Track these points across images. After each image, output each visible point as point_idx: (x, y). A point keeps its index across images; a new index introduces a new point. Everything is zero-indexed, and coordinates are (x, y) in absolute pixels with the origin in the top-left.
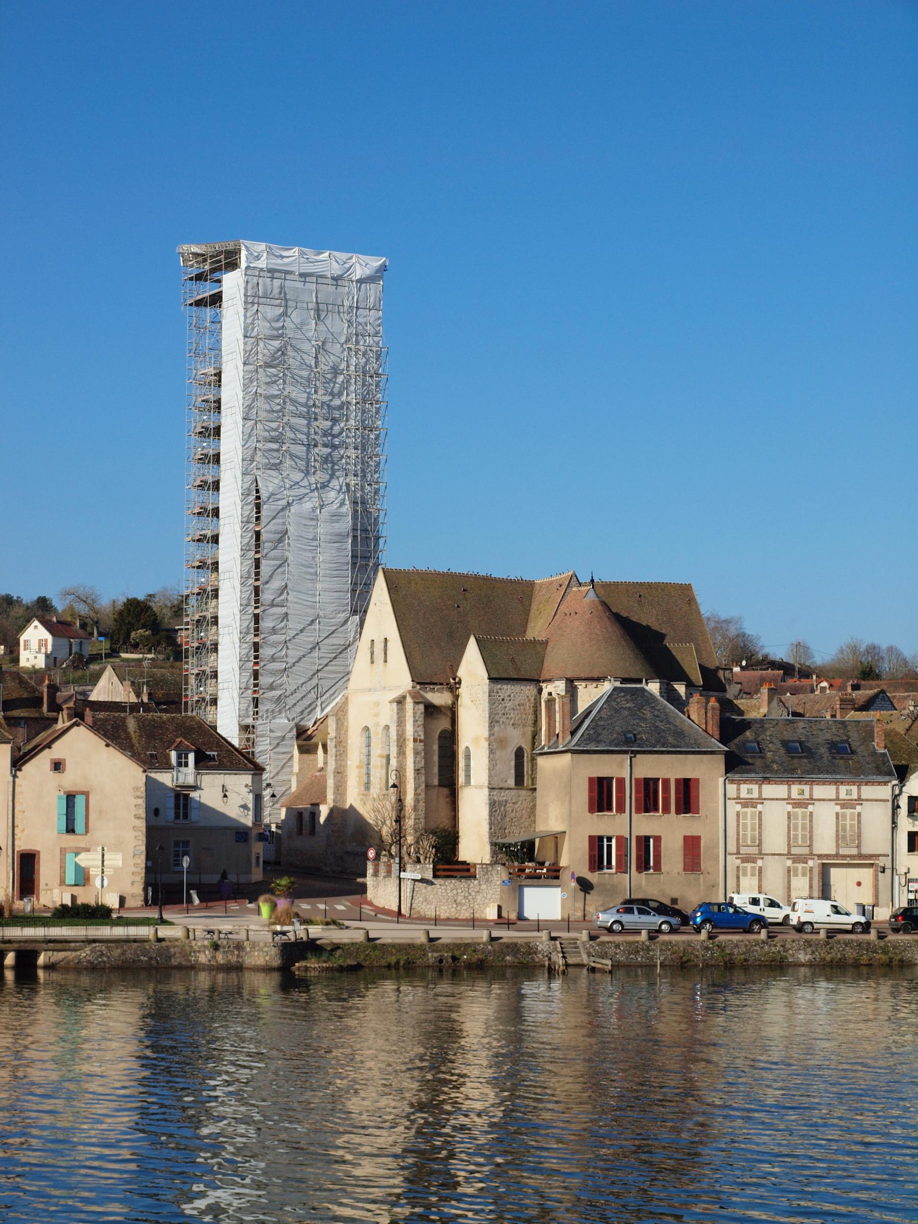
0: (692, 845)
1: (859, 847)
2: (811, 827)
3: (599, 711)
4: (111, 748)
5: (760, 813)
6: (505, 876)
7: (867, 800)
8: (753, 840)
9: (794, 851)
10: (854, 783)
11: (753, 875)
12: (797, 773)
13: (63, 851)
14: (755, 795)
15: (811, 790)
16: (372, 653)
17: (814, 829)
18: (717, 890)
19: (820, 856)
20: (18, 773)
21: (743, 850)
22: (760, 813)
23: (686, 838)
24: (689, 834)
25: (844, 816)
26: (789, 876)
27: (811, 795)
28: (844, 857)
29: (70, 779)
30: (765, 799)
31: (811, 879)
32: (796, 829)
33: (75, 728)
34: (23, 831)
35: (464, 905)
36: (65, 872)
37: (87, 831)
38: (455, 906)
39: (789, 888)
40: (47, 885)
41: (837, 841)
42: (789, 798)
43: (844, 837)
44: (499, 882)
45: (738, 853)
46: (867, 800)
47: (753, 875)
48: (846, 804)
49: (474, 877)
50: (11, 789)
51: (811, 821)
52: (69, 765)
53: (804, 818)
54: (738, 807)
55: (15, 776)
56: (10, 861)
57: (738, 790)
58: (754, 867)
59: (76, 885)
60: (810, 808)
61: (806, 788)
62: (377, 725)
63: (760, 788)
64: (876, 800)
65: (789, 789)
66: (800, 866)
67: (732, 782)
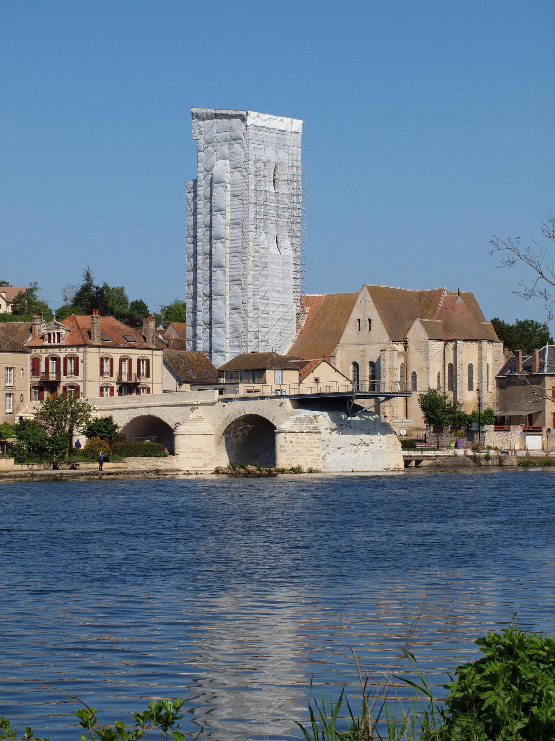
6: (521, 431)
49: (509, 431)
62: (363, 361)
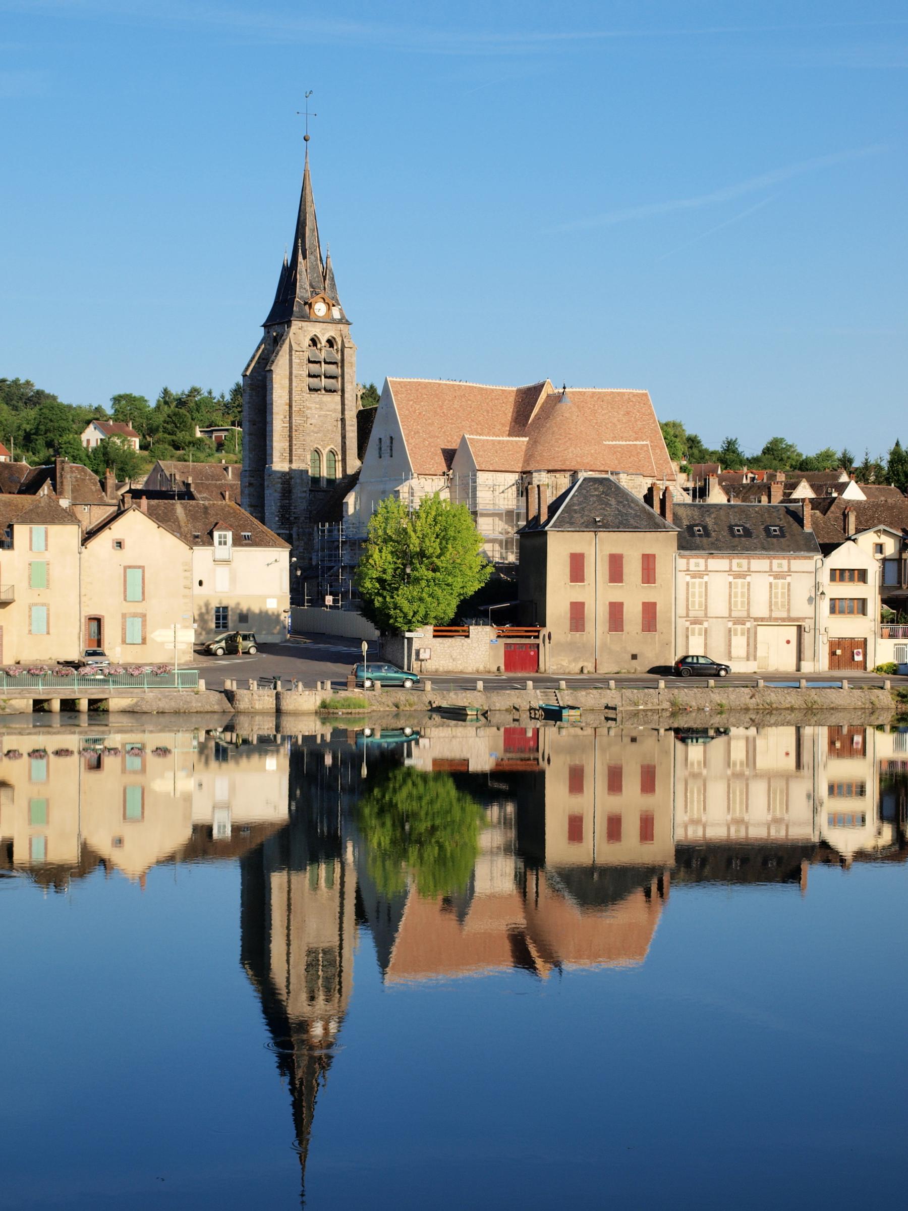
0: (649, 611)
1: (789, 610)
2: (749, 595)
3: (571, 498)
5: (706, 583)
7: (796, 572)
8: (700, 606)
9: (734, 614)
10: (784, 558)
11: (700, 634)
12: (737, 550)
14: (702, 568)
15: (749, 564)
16: (380, 449)
17: (751, 597)
18: (670, 647)
19: (756, 619)
21: (691, 614)
22: (706, 583)
23: (644, 604)
24: (646, 601)
25: (777, 587)
26: (730, 635)
27: (749, 568)
28: (776, 619)
29: (128, 556)
30: (710, 571)
31: (748, 638)
32: (736, 597)
35: (459, 660)
36: (125, 633)
37: (144, 599)
38: (451, 661)
39: (730, 645)
41: (770, 606)
42: (731, 570)
43: (776, 603)
44: (488, 641)
45: (687, 616)
46: (796, 572)
47: (700, 634)
48: (777, 576)
49: (468, 636)
51: (749, 589)
52: (127, 544)
53: (743, 586)
54: (688, 578)
57: (688, 563)
58: (701, 628)
60: (748, 579)
61: (744, 562)
63: (706, 562)
64: (803, 572)
65: (731, 563)
66: (739, 627)
67: (682, 557)
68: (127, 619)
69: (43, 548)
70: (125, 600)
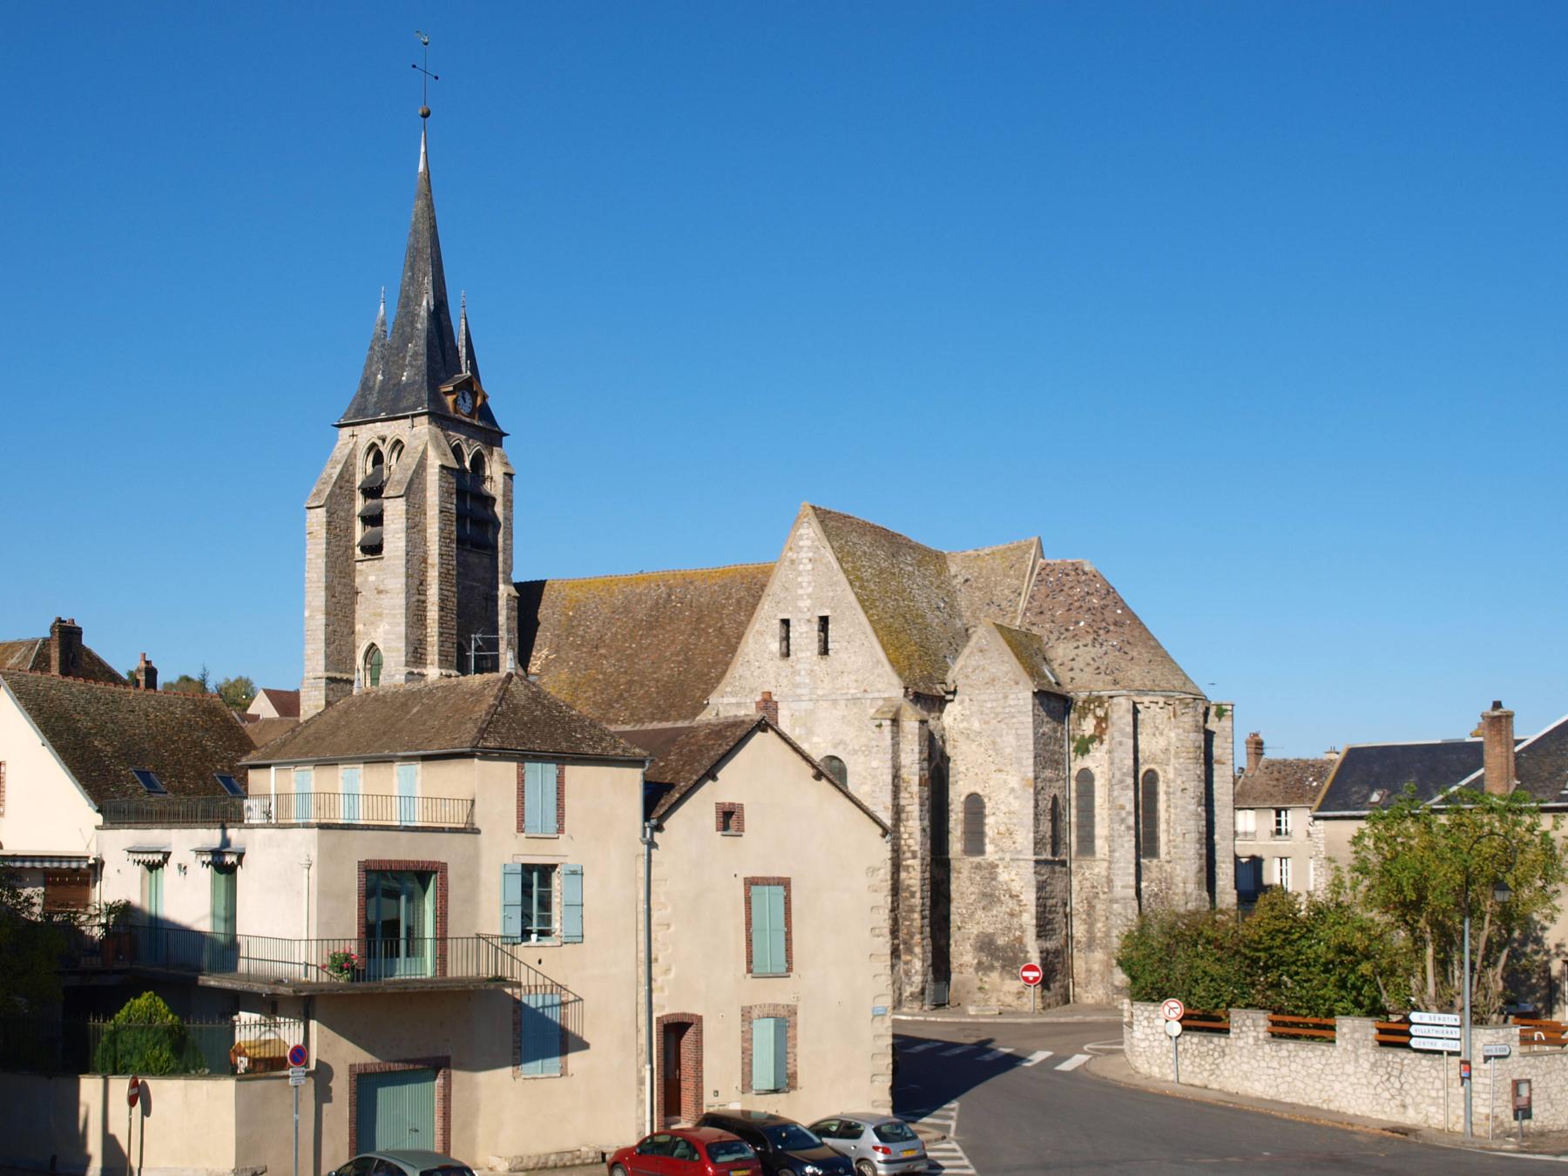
4: (824, 782)
13: (747, 1015)
20: (658, 837)
33: (759, 735)
34: (668, 971)
36: (750, 1064)
40: (716, 1093)
50: (642, 873)
55: (652, 845)
56: (643, 1040)
59: (776, 1091)
68: (756, 1023)
69: (553, 825)
70: (750, 971)
